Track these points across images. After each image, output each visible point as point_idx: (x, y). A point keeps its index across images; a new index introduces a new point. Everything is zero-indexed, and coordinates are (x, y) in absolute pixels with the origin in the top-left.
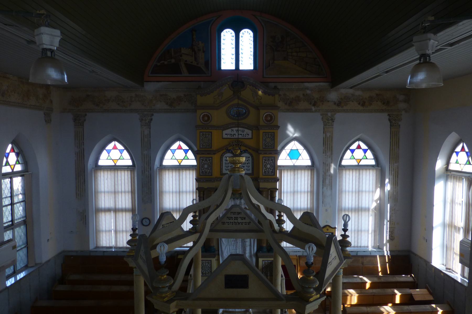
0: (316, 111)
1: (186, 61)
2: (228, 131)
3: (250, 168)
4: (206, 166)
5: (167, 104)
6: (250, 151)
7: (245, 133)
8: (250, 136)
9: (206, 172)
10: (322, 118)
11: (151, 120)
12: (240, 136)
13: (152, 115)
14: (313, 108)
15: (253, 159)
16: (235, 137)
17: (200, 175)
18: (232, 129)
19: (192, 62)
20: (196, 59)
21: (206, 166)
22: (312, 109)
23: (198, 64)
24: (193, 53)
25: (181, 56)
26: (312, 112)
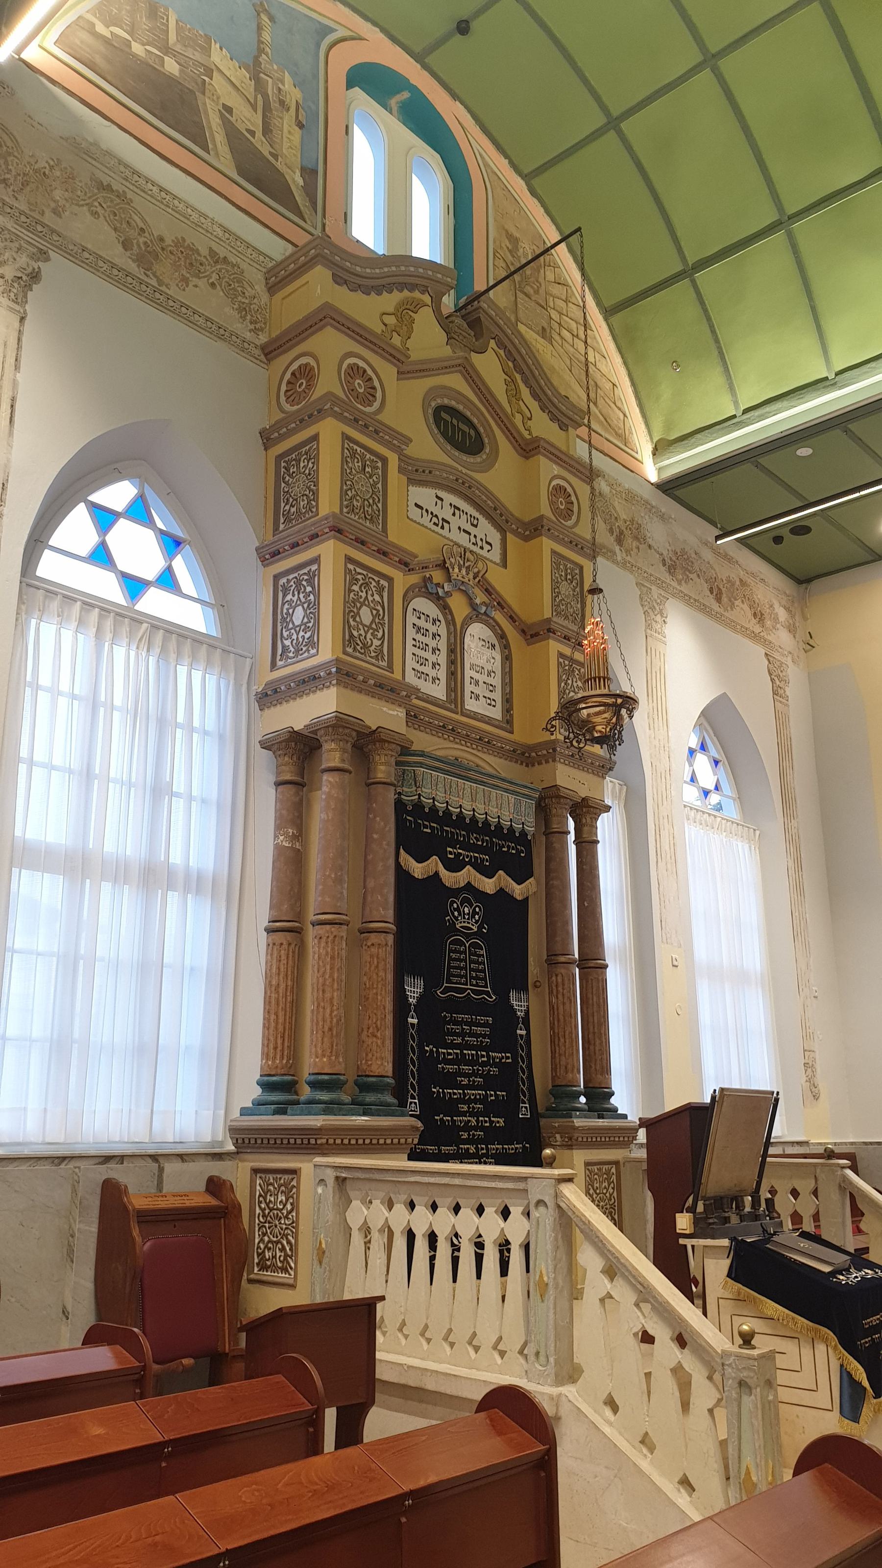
0: (624, 565)
1: (229, 110)
2: (424, 495)
3: (497, 696)
4: (366, 615)
5: (126, 245)
6: (498, 616)
7: (479, 532)
8: (495, 555)
9: (365, 646)
10: (641, 599)
11: (35, 276)
12: (463, 540)
13: (43, 255)
14: (617, 549)
15: (507, 658)
16: (445, 532)
17: (345, 653)
18: (441, 494)
19: (253, 133)
20: (267, 130)
21: (366, 615)
22: (615, 553)
23: (275, 156)
24: (259, 96)
25: (209, 72)
26: (616, 563)
